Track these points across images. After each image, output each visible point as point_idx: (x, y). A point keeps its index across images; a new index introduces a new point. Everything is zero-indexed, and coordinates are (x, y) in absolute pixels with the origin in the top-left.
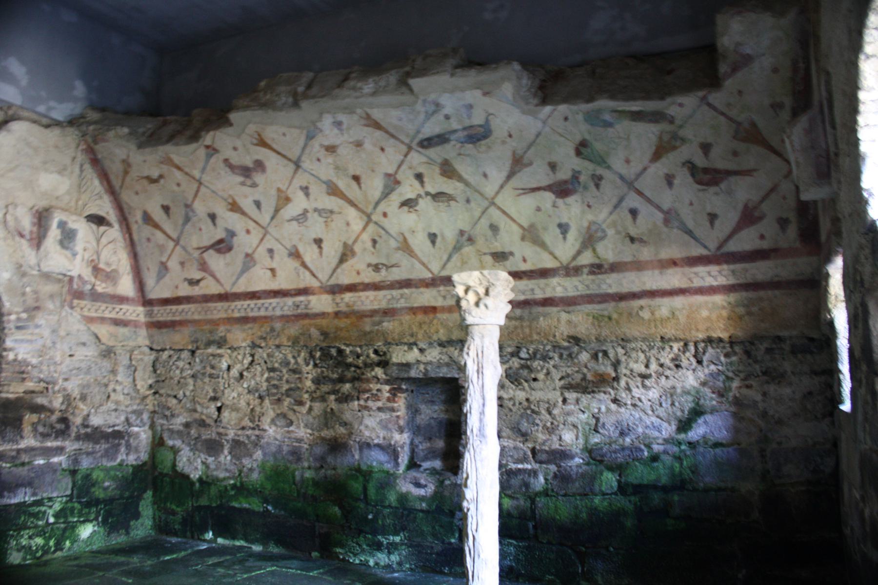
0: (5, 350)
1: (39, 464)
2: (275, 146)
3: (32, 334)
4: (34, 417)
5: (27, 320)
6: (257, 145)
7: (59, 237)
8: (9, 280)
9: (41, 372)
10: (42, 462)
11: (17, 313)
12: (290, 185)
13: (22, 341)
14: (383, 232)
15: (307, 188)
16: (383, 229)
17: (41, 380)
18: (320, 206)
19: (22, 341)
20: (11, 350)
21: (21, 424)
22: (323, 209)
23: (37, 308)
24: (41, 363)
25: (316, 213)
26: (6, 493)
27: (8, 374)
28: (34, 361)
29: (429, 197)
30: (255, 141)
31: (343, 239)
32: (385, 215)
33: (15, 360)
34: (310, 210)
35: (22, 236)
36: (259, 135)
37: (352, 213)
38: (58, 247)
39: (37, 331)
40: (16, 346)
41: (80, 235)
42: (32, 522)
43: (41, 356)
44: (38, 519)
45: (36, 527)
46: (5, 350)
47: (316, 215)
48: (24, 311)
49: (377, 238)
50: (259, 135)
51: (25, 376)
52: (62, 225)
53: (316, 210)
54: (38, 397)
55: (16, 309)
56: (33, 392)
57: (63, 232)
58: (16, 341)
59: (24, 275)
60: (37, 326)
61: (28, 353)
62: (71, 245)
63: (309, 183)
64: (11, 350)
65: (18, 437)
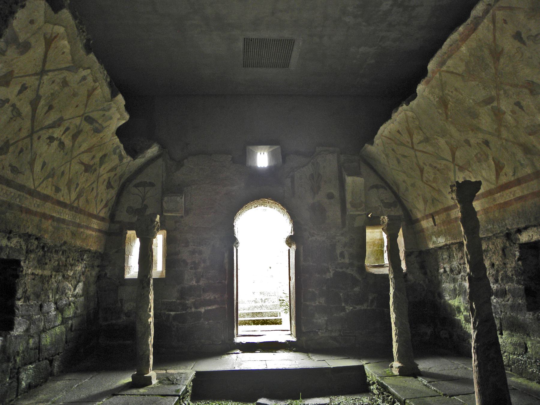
2: (50, 52)
6: (45, 38)
12: (21, 77)
14: (30, 147)
15: (26, 88)
16: (32, 145)
18: (18, 104)
22: (18, 109)
25: (12, 108)
29: (59, 142)
30: (48, 36)
31: (10, 137)
32: (39, 138)
34: (10, 103)
36: (55, 37)
37: (27, 124)
47: (11, 108)
49: (24, 149)
50: (55, 37)
53: (14, 105)
63: (31, 86)
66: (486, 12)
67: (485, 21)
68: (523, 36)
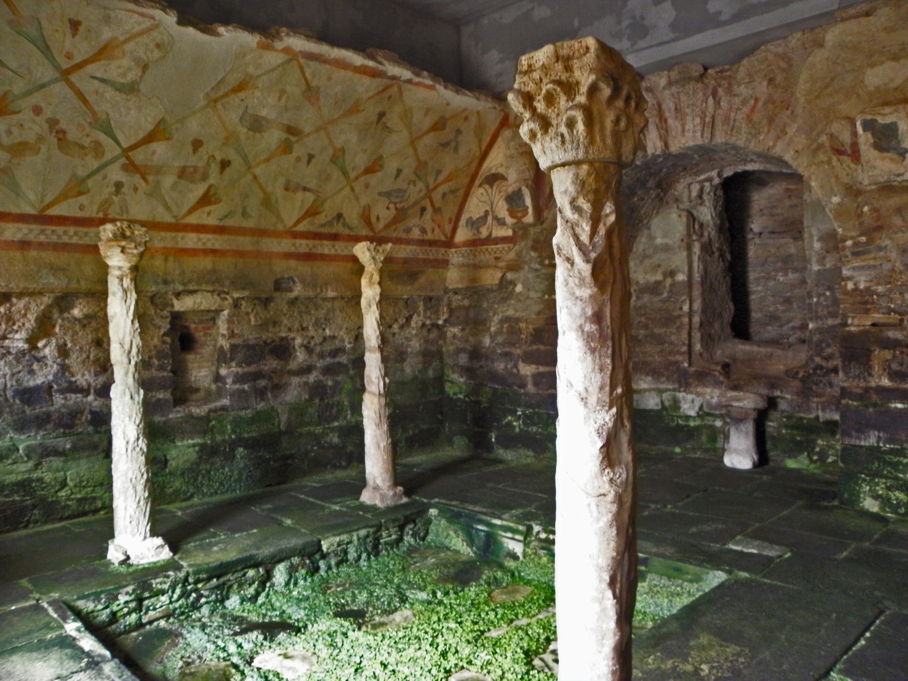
0: (843, 279)
1: (896, 408)
3: (875, 259)
4: (888, 354)
5: (867, 243)
7: (872, 141)
8: (839, 204)
9: (891, 300)
10: (900, 406)
11: (852, 238)
13: (862, 268)
17: (890, 311)
19: (862, 268)
20: (849, 278)
21: (869, 360)
23: (880, 228)
24: (890, 291)
26: (854, 433)
27: (848, 305)
28: (880, 289)
33: (856, 289)
35: (839, 152)
38: (876, 153)
39: (881, 254)
40: (854, 274)
41: (902, 126)
42: (889, 472)
43: (889, 283)
44: (897, 470)
45: (896, 479)
46: (843, 279)
48: (861, 235)
51: (869, 306)
52: (869, 126)
54: (889, 330)
55: (853, 234)
56: (884, 325)
57: (873, 135)
58: (854, 268)
59: (859, 193)
60: (880, 249)
61: (871, 281)
62: (893, 143)
64: (849, 278)
65: (866, 374)
66: (394, 78)
67: (385, 80)
68: (384, 120)
